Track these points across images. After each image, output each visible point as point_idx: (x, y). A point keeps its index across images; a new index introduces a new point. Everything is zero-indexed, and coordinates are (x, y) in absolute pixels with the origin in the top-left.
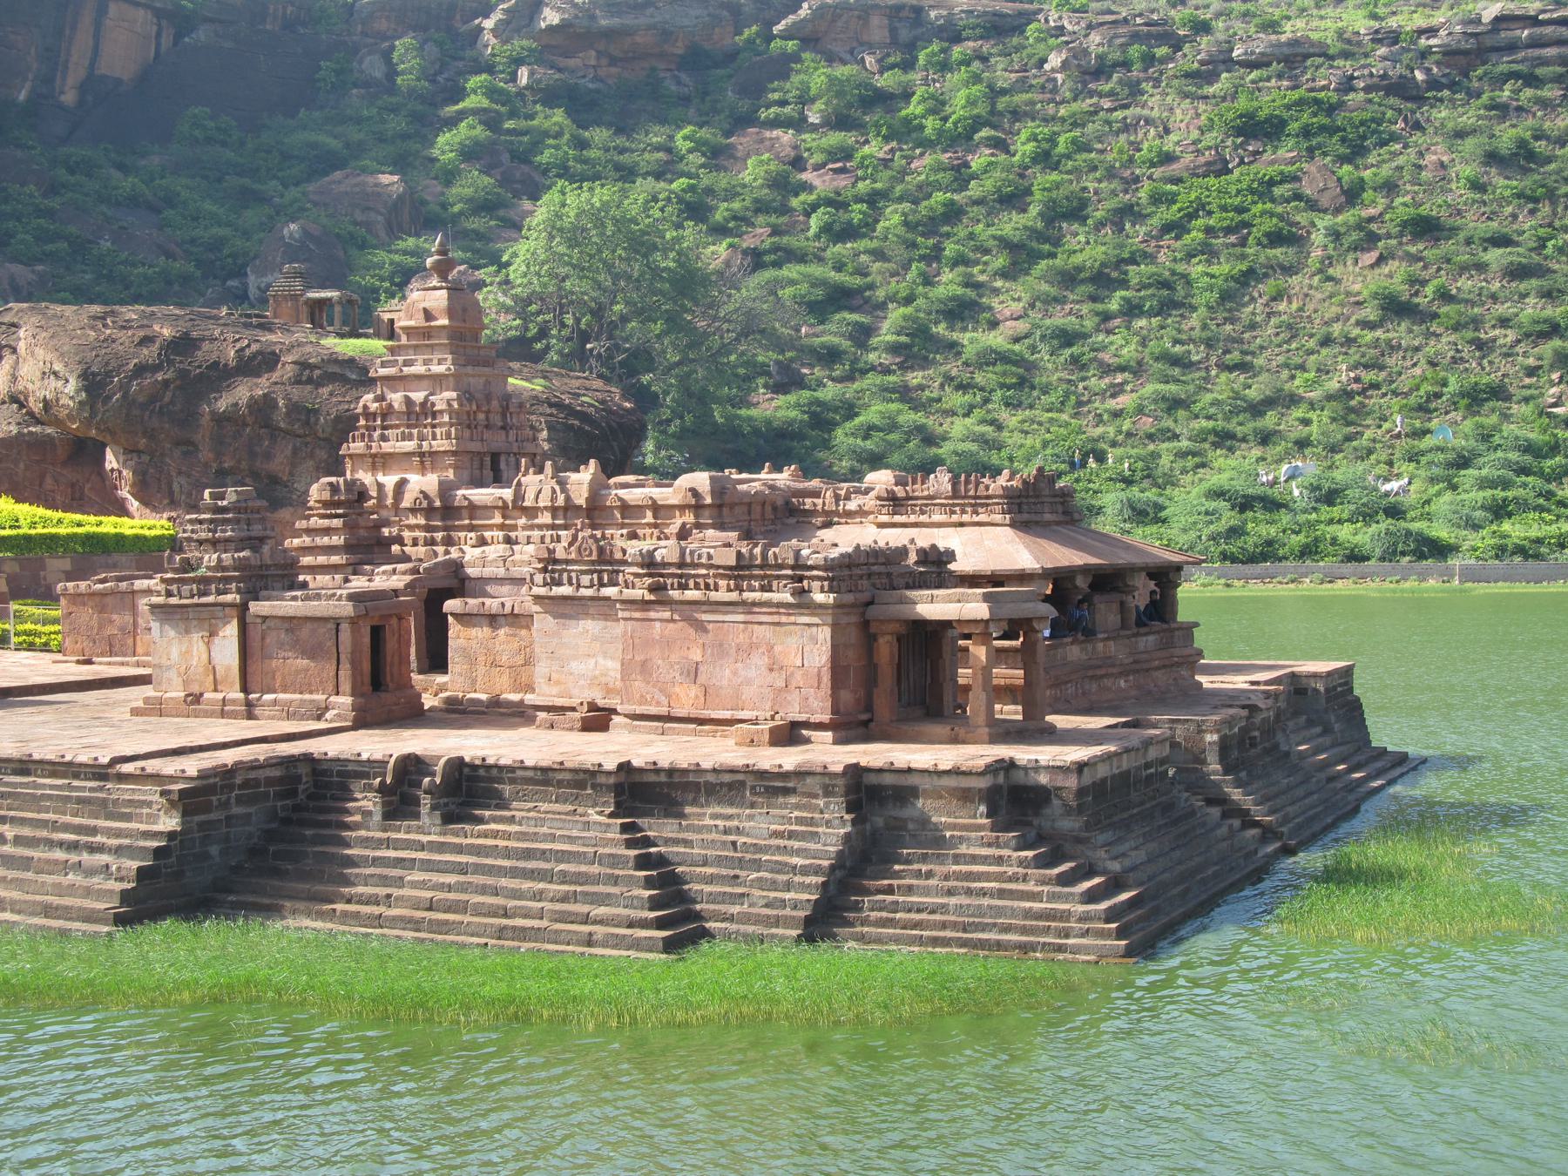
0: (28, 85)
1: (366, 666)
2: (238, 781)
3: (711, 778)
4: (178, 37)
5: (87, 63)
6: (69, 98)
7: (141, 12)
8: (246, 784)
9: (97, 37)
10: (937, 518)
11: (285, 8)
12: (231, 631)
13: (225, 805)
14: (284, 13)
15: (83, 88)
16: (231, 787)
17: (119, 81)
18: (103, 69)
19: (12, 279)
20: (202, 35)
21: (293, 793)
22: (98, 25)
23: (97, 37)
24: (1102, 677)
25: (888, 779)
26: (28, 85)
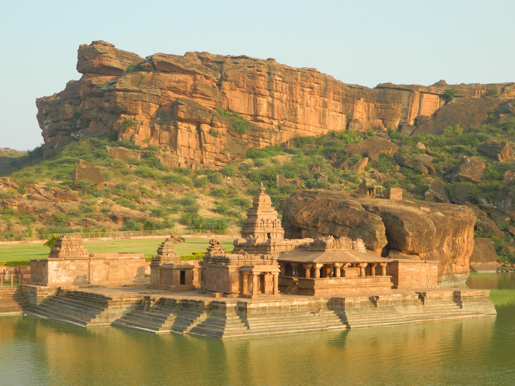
0: (399, 120)
1: (179, 279)
2: (124, 300)
3: (191, 303)
4: (446, 102)
5: (417, 112)
6: (412, 123)
7: (434, 96)
8: (126, 301)
9: (420, 104)
10: (316, 249)
11: (481, 91)
12: (159, 271)
13: (121, 304)
14: (481, 93)
15: (416, 120)
16: (123, 301)
17: (428, 117)
18: (422, 113)
19: (379, 177)
20: (454, 100)
21: (141, 303)
22: (420, 100)
23: (420, 104)
24: (343, 288)
25: (215, 304)
26: (399, 120)
